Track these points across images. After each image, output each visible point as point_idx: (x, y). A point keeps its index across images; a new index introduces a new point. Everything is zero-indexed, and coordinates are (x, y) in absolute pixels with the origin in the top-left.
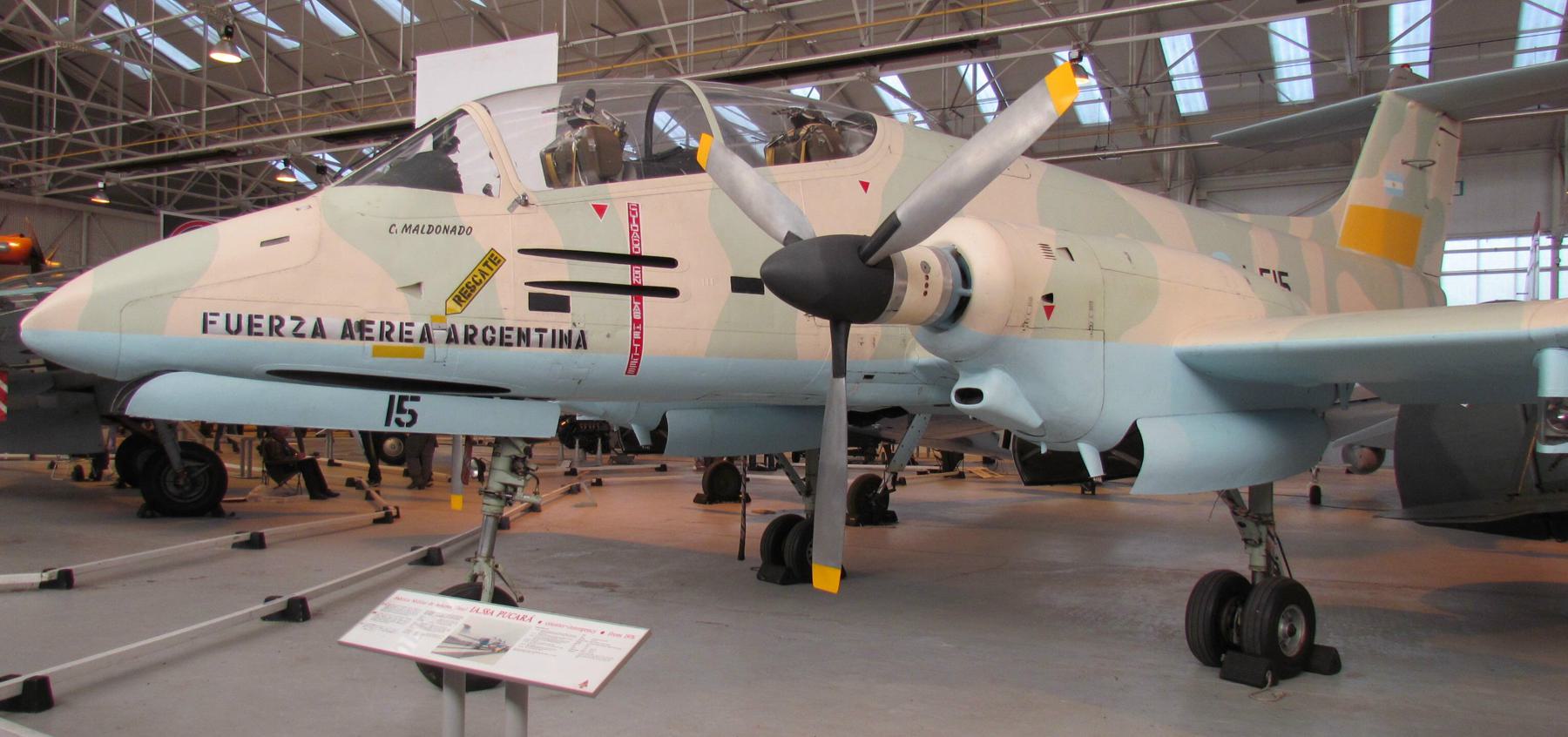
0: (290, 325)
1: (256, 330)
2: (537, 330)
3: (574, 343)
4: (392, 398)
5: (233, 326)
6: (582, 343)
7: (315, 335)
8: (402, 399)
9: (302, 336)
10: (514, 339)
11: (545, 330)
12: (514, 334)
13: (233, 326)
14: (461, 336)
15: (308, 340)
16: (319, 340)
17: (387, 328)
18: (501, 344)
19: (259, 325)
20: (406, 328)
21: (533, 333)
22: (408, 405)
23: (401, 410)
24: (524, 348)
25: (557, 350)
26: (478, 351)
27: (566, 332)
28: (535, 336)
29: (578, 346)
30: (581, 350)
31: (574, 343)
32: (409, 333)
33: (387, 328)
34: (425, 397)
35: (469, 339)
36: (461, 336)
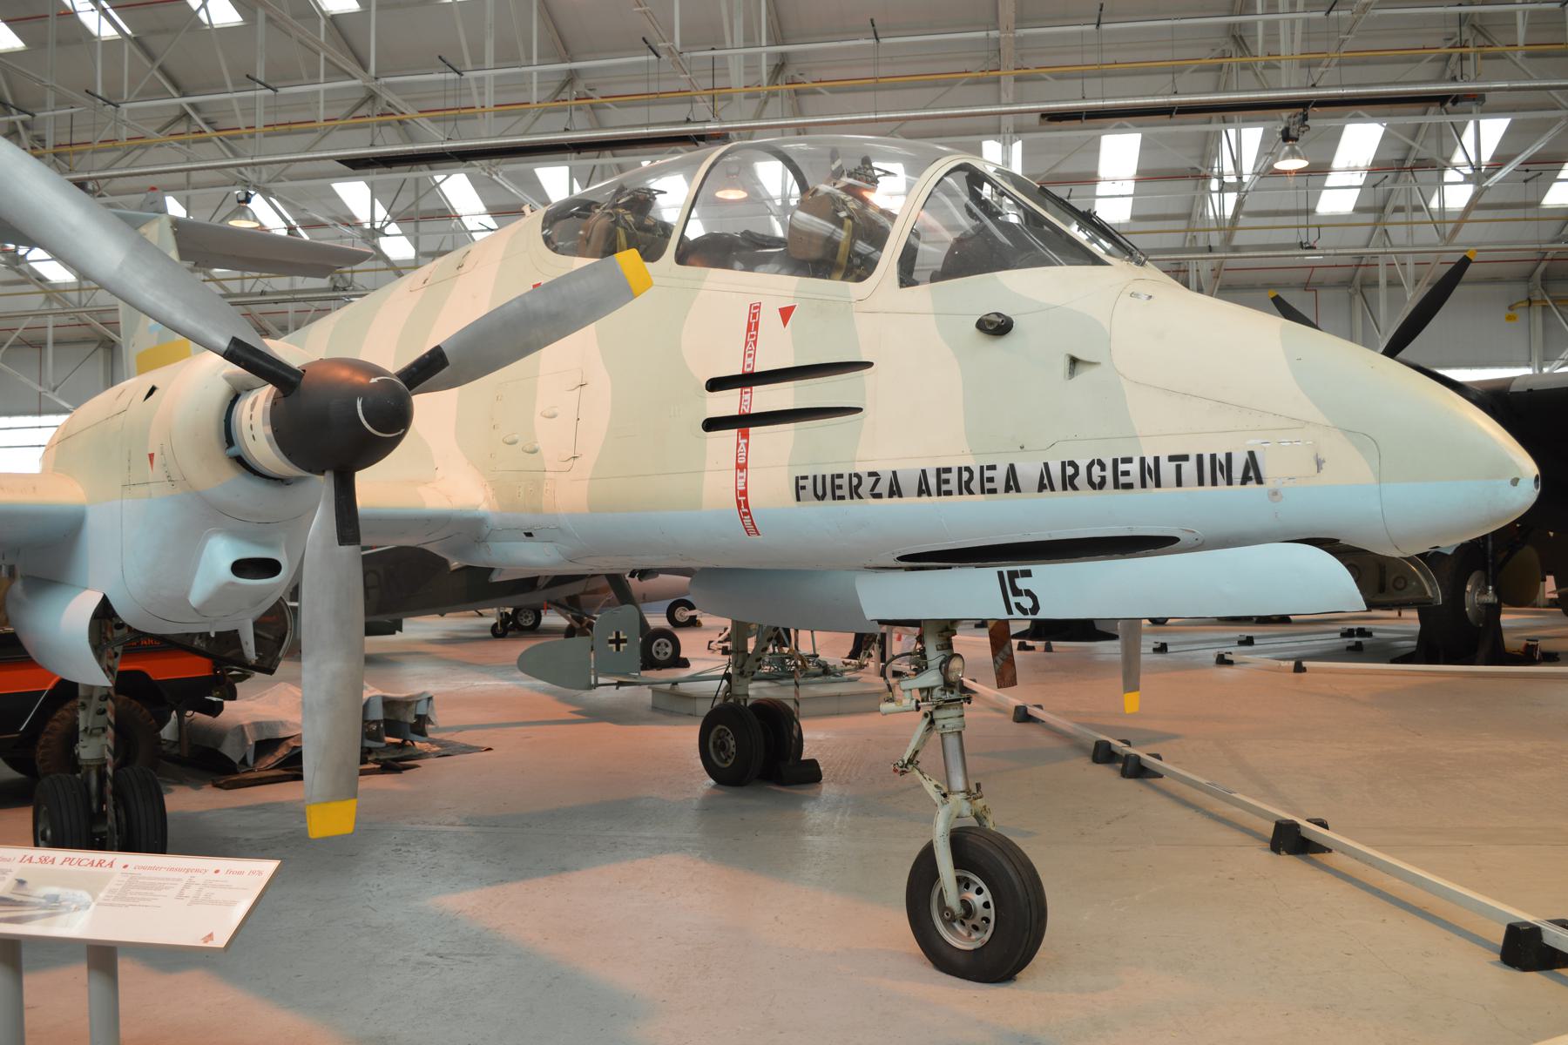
0: (868, 482)
1: (838, 493)
2: (1172, 458)
3: (1237, 473)
4: (1000, 574)
5: (820, 493)
6: (1252, 473)
7: (1008, 489)
8: (1013, 575)
9: (879, 496)
10: (1135, 477)
11: (1185, 458)
12: (1134, 468)
13: (820, 493)
14: (1057, 481)
15: (886, 501)
16: (896, 499)
17: (966, 475)
18: (1116, 486)
19: (840, 487)
20: (988, 474)
21: (1164, 462)
22: (1021, 583)
23: (1017, 592)
24: (1151, 489)
25: (1208, 488)
26: (1084, 498)
27: (1221, 457)
28: (1168, 469)
30: (1252, 485)
31: (1237, 473)
32: (991, 480)
33: (966, 475)
34: (1036, 569)
35: (1069, 483)
36: (1057, 481)
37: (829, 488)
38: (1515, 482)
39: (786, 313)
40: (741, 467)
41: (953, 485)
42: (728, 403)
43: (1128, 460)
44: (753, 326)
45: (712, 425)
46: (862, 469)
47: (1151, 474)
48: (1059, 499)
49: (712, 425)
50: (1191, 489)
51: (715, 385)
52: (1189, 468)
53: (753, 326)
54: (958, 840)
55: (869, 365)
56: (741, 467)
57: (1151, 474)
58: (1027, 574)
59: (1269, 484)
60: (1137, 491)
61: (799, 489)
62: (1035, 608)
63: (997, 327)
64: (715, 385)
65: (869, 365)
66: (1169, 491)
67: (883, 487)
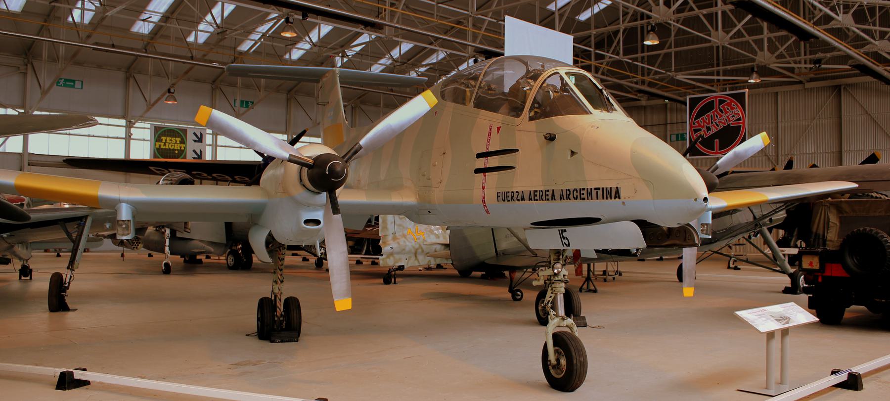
0: (516, 195)
2: (596, 189)
6: (617, 195)
10: (585, 196)
11: (598, 189)
12: (585, 192)
28: (594, 192)
29: (615, 198)
30: (617, 200)
35: (568, 197)
37: (507, 197)
38: (696, 200)
39: (499, 129)
40: (483, 188)
41: (537, 197)
42: (481, 163)
43: (583, 189)
44: (490, 134)
45: (477, 171)
46: (514, 190)
47: (590, 194)
48: (565, 203)
49: (477, 171)
50: (601, 200)
51: (479, 156)
52: (600, 192)
53: (490, 134)
54: (555, 336)
55: (517, 150)
56: (483, 188)
57: (590, 194)
58: (565, 231)
59: (622, 199)
60: (586, 200)
61: (498, 197)
62: (569, 245)
63: (551, 138)
64: (479, 156)
65: (517, 150)
66: (595, 201)
67: (520, 197)
